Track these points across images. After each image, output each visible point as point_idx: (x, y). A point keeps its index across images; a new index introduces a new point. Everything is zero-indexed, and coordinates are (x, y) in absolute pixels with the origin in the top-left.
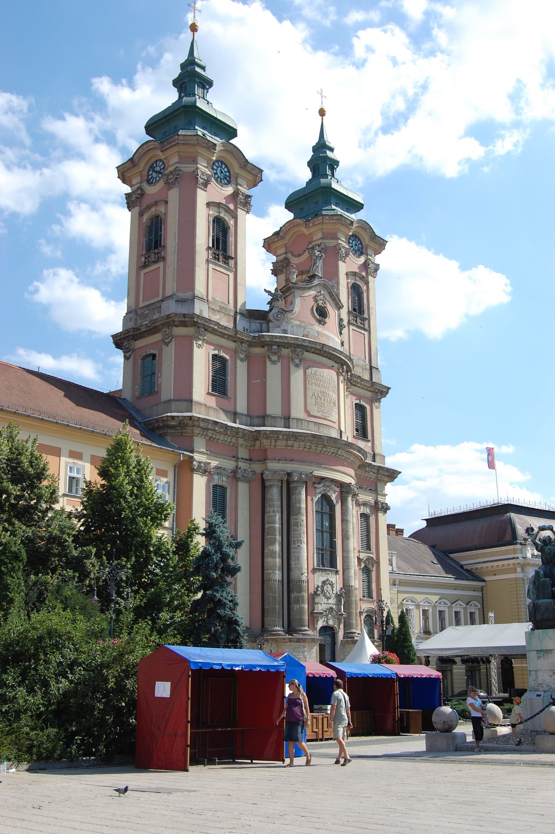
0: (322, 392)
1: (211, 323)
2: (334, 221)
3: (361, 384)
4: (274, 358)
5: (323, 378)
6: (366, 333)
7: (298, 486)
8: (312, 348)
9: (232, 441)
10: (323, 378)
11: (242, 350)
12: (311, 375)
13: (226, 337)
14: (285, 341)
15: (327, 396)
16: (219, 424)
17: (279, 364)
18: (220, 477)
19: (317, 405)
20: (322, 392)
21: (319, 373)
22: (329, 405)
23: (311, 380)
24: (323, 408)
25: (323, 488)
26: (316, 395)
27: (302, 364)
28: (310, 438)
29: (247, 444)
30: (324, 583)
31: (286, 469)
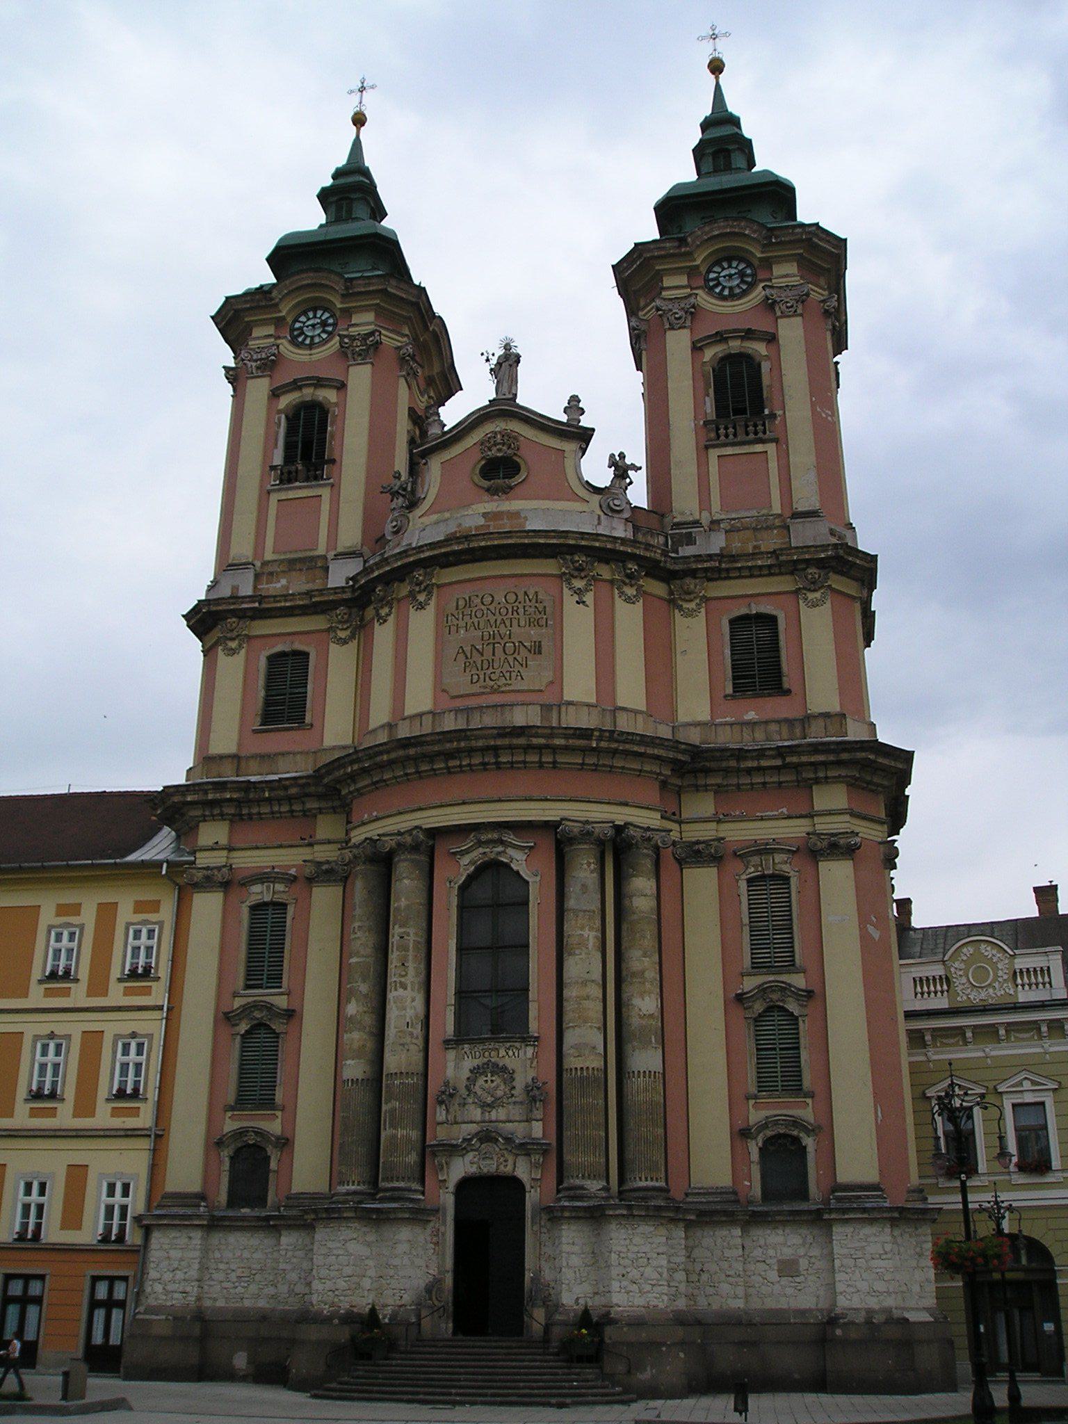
0: (486, 637)
1: (243, 603)
2: (638, 263)
3: (739, 569)
4: (383, 612)
5: (492, 607)
6: (771, 448)
7: (399, 861)
8: (446, 554)
9: (294, 807)
10: (492, 607)
11: (340, 622)
12: (455, 613)
13: (297, 612)
14: (388, 568)
15: (506, 639)
16: (229, 786)
17: (391, 619)
18: (268, 888)
19: (467, 671)
20: (486, 637)
21: (479, 600)
22: (511, 659)
23: (455, 622)
24: (491, 670)
25: (481, 850)
26: (467, 649)
27: (433, 598)
28: (401, 753)
29: (330, 804)
30: (476, 1072)
31: (368, 835)
